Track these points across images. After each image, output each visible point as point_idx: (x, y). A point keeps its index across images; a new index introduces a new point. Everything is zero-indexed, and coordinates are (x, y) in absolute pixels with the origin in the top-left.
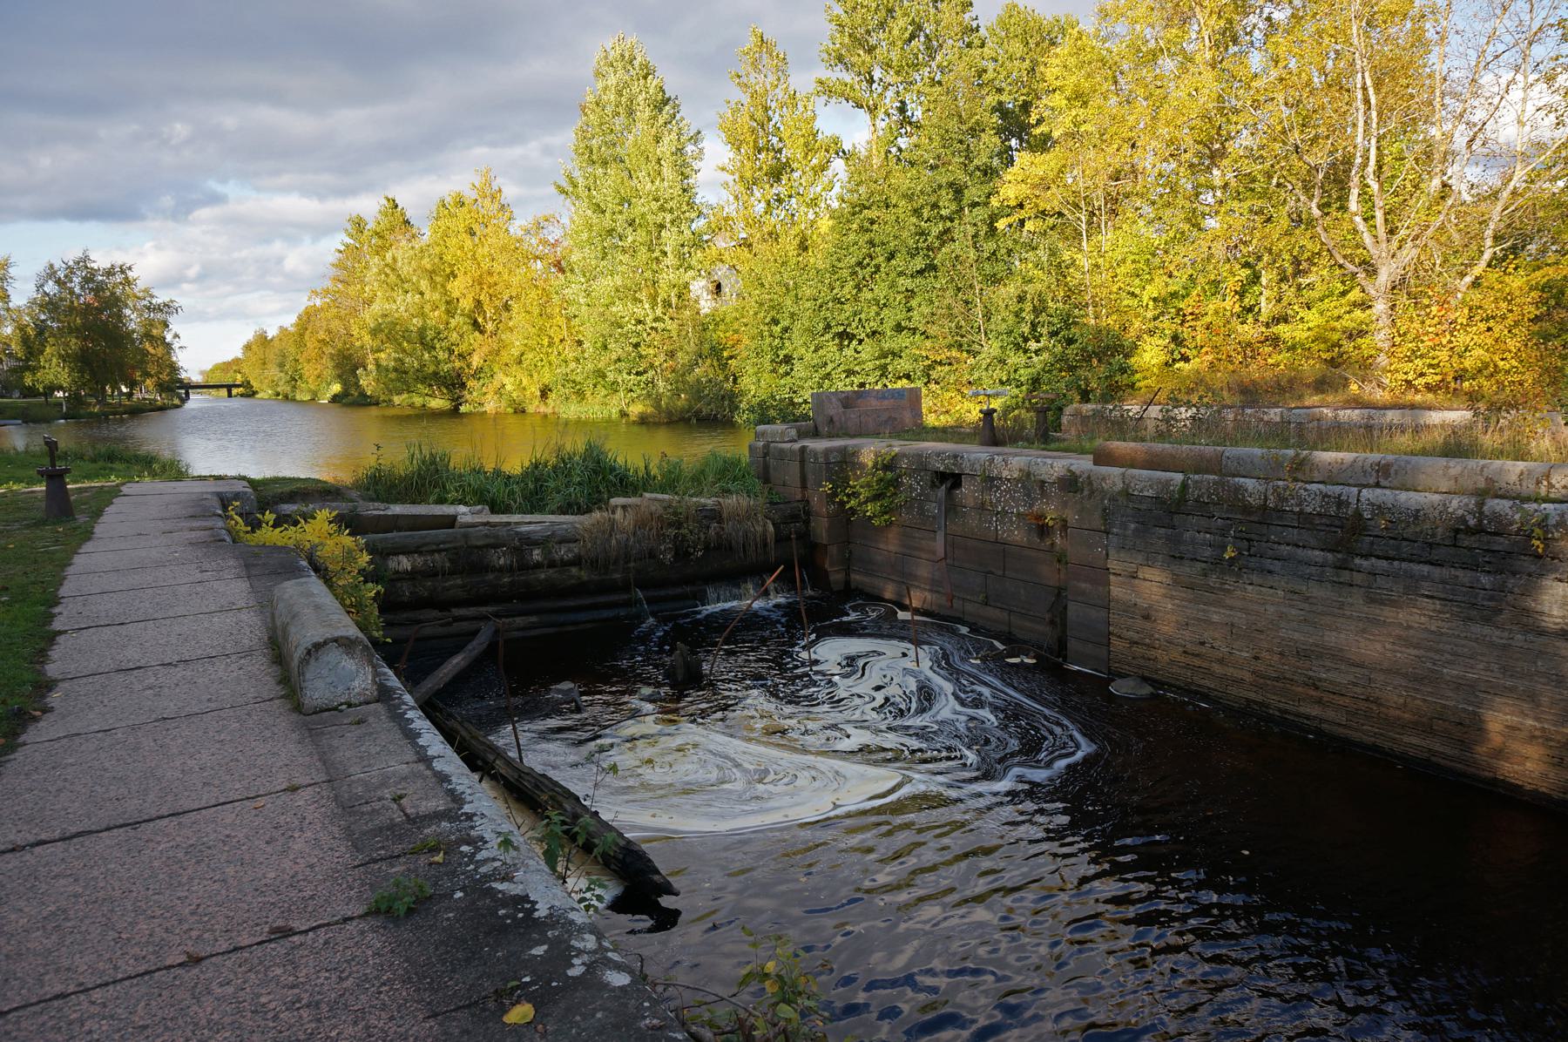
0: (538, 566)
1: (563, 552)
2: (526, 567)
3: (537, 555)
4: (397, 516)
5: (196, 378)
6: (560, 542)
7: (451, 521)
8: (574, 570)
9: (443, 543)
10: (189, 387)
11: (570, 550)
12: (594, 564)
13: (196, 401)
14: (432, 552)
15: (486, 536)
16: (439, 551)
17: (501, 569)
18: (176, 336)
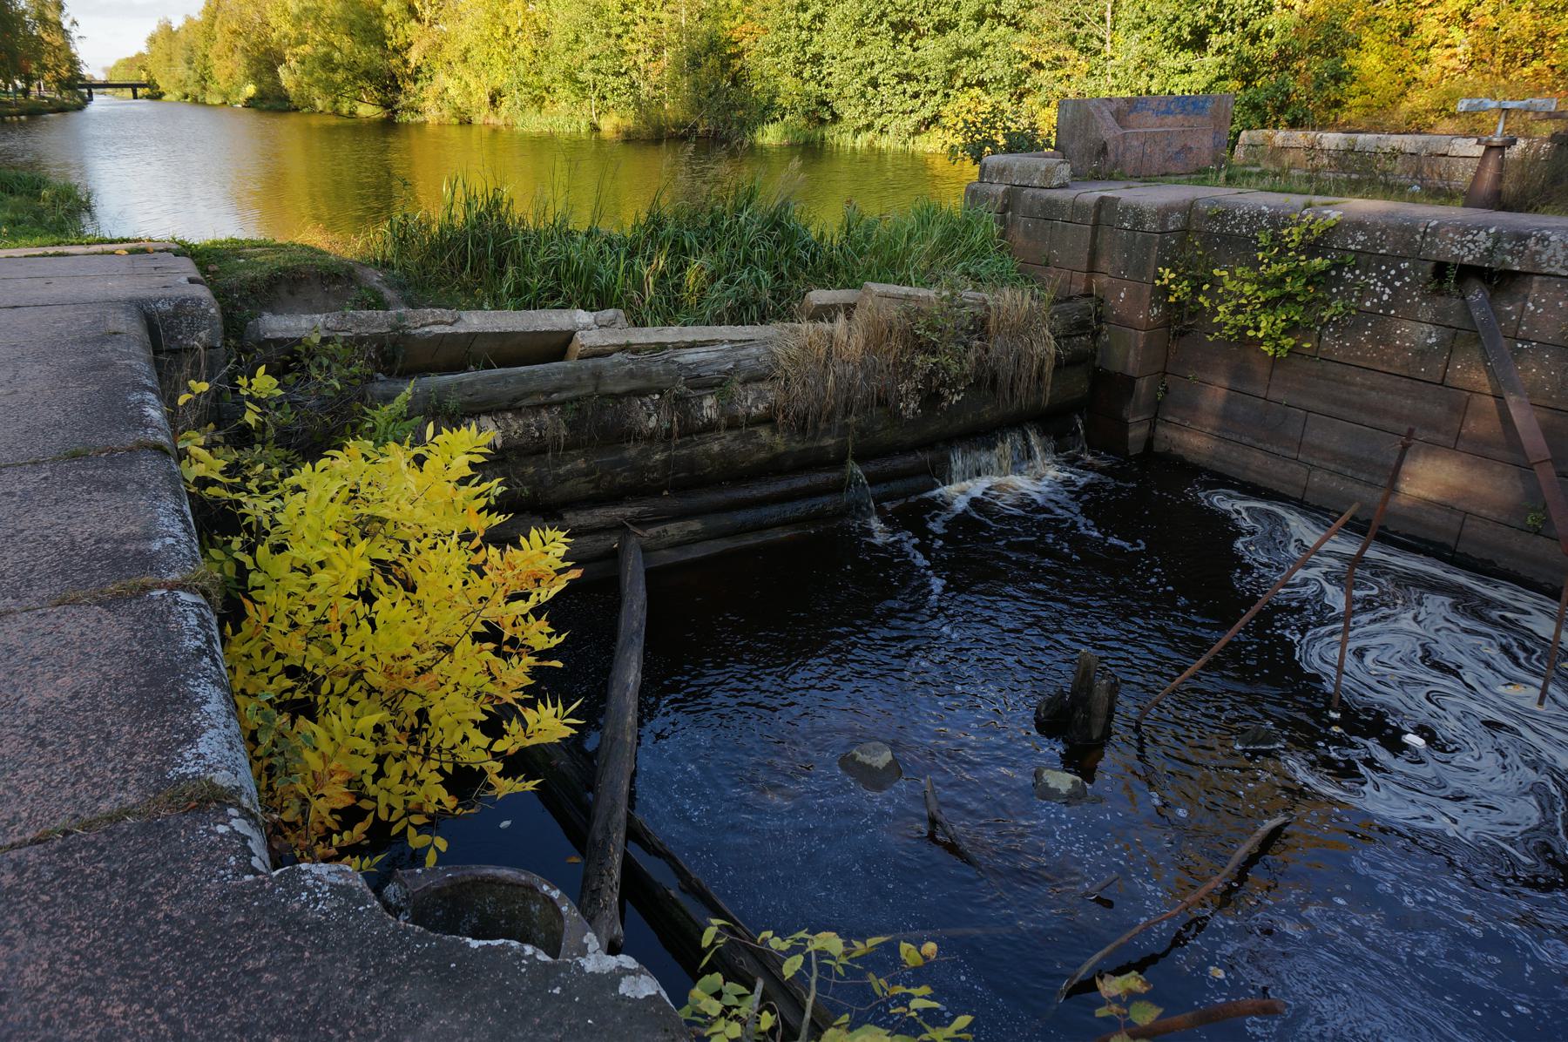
0: (711, 427)
1: (751, 402)
2: (692, 430)
3: (709, 407)
4: (473, 337)
5: (100, 77)
6: (745, 382)
7: (557, 346)
8: (764, 433)
9: (559, 390)
10: (92, 86)
11: (760, 397)
12: (802, 424)
13: (100, 103)
14: (536, 408)
15: (631, 375)
16: (549, 406)
17: (651, 437)
18: (74, 23)
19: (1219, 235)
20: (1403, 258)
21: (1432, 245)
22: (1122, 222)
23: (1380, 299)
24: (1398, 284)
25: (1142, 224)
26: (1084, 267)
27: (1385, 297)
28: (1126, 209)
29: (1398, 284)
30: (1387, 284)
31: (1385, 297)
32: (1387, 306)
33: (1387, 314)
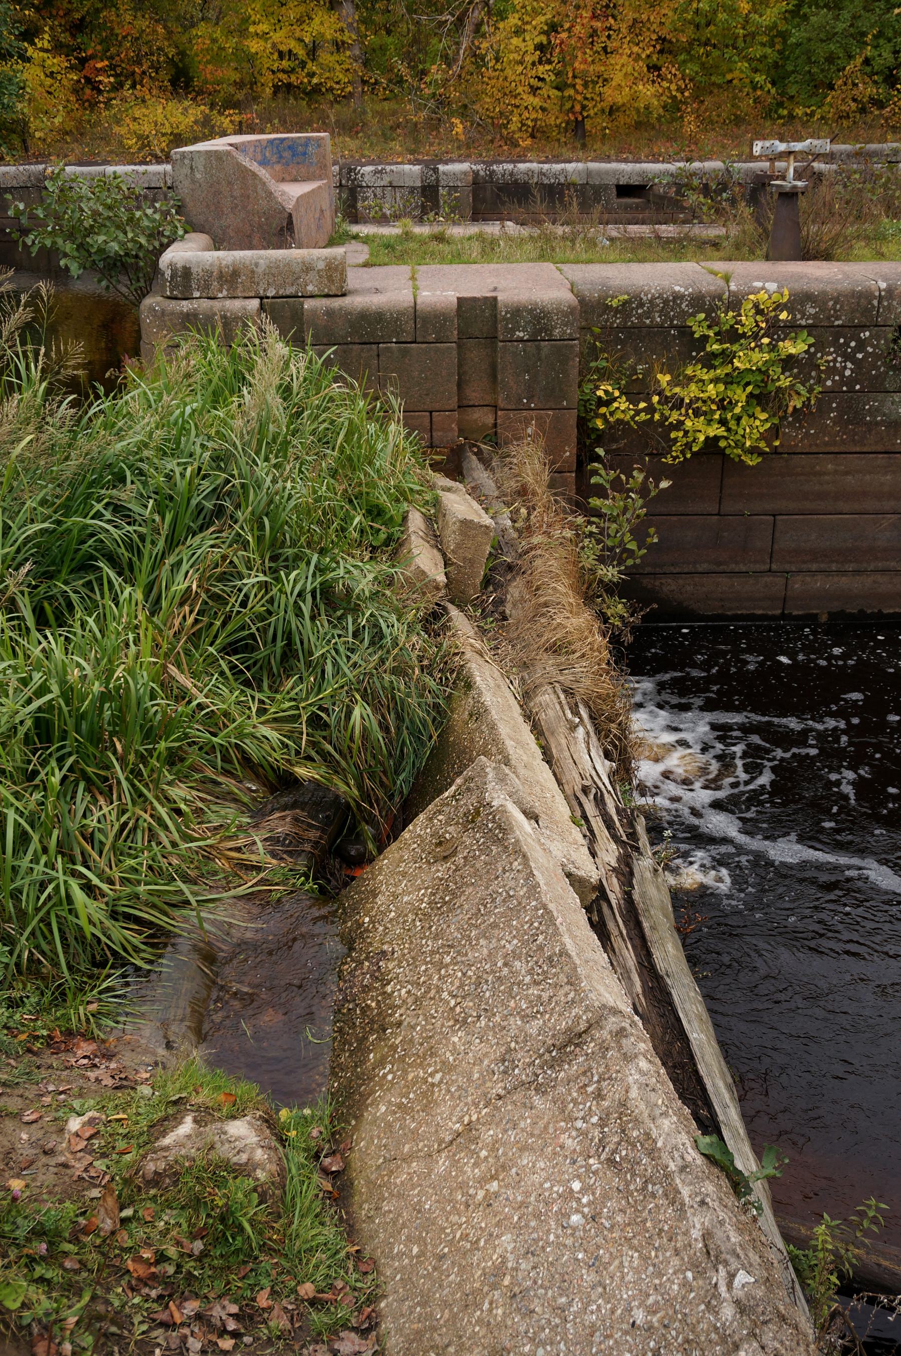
19: (621, 328)
20: (863, 327)
21: (889, 308)
22: (513, 330)
23: (842, 376)
24: (860, 356)
25: (548, 329)
26: (454, 402)
27: (848, 373)
28: (517, 312)
29: (860, 356)
30: (847, 357)
31: (848, 373)
32: (850, 382)
33: (851, 390)
